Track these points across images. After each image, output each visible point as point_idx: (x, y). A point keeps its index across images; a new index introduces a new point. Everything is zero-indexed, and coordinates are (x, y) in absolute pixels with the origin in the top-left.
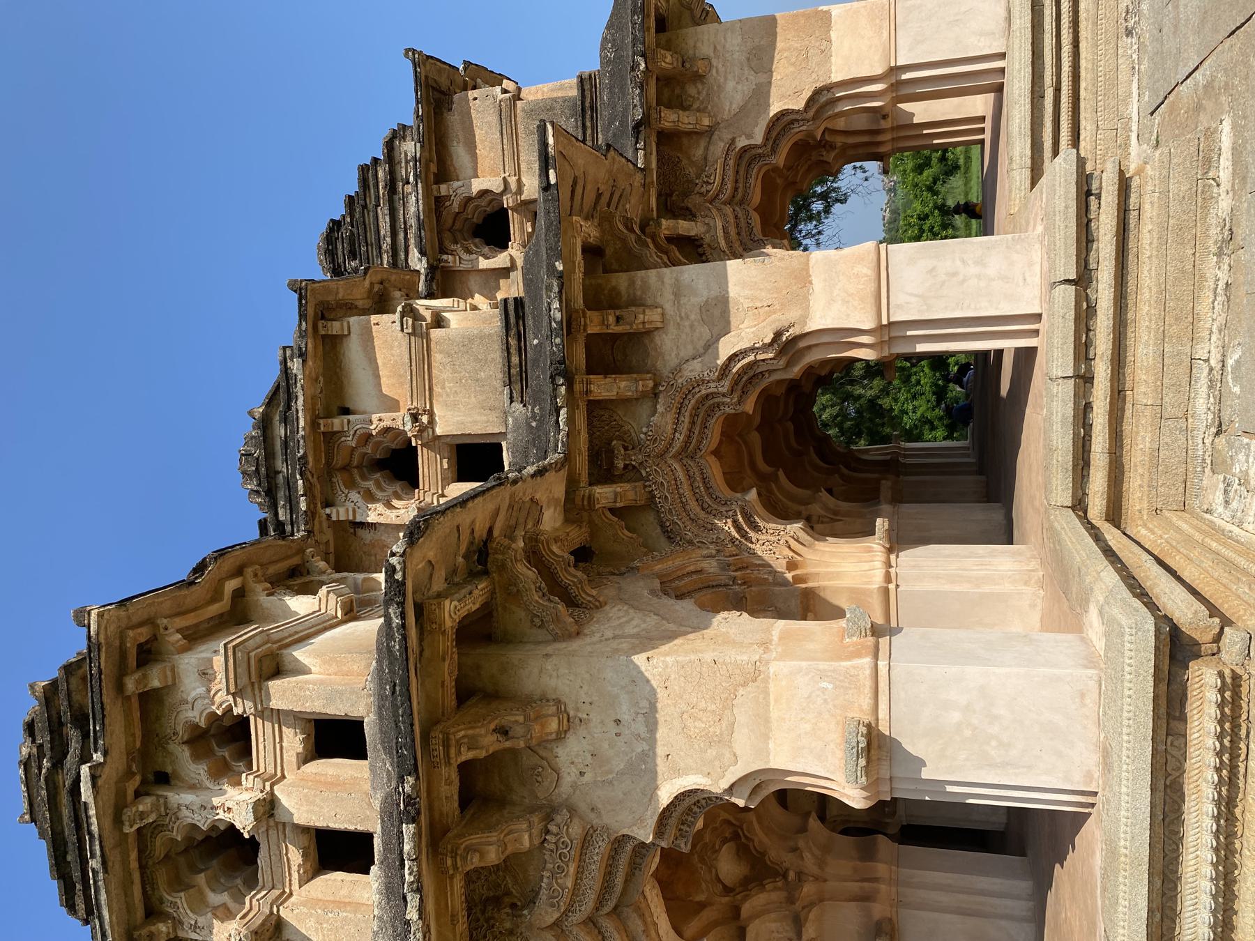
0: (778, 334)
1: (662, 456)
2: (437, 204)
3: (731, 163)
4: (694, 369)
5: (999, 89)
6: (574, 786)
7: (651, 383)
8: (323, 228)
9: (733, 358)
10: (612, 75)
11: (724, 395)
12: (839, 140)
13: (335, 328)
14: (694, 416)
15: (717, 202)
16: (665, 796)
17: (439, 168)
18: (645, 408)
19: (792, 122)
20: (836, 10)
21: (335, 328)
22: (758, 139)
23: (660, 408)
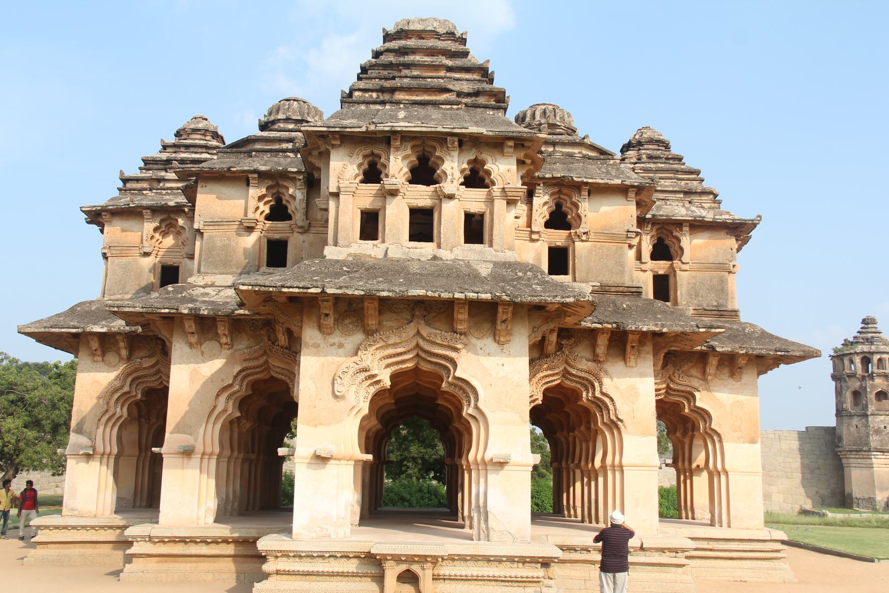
0: (621, 421)
1: (567, 362)
2: (679, 224)
3: (688, 389)
4: (606, 381)
5: (712, 524)
6: (475, 345)
7: (601, 360)
8: (665, 137)
9: (612, 400)
10: (738, 330)
11: (594, 393)
12: (687, 441)
13: (632, 195)
14: (583, 378)
15: (669, 381)
16: (474, 383)
17: (698, 226)
18: (587, 354)
19: (705, 421)
20: (758, 446)
21: (632, 195)
22: (698, 404)
23: (589, 363)
